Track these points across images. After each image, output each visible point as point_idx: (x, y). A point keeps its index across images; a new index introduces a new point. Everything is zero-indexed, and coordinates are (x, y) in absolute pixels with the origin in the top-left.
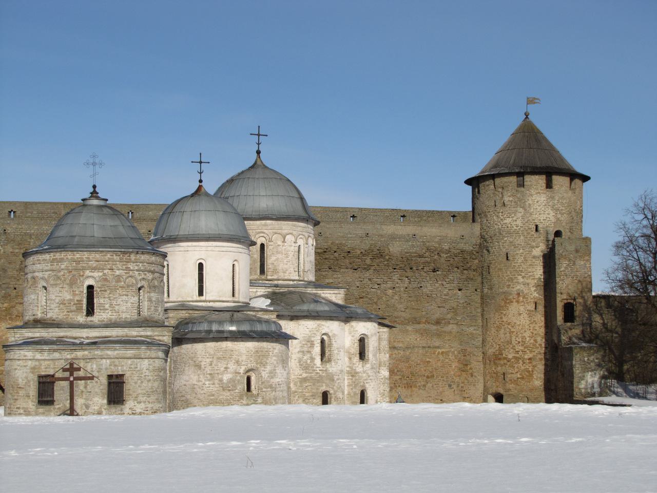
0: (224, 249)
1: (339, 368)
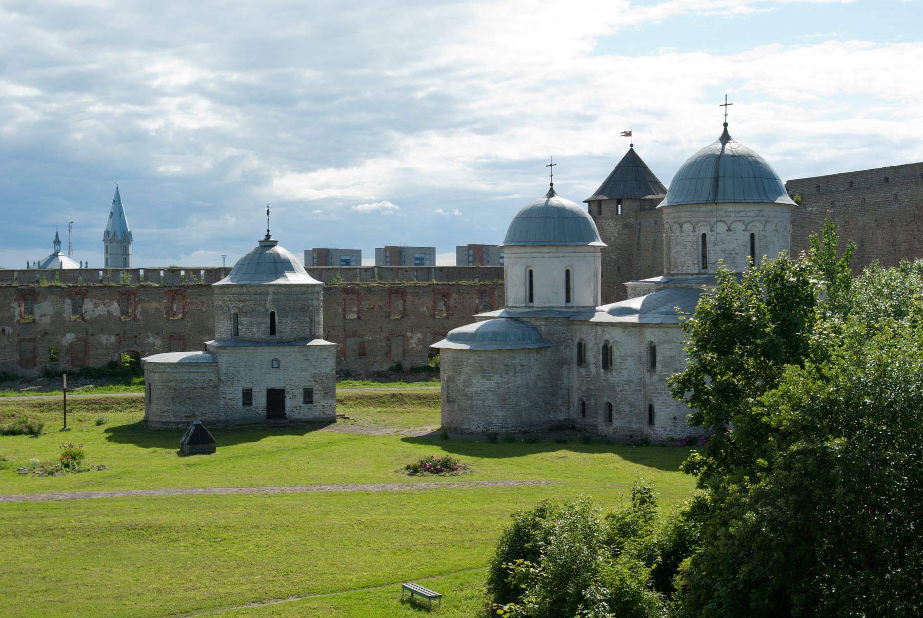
0: (518, 255)
1: (626, 377)
